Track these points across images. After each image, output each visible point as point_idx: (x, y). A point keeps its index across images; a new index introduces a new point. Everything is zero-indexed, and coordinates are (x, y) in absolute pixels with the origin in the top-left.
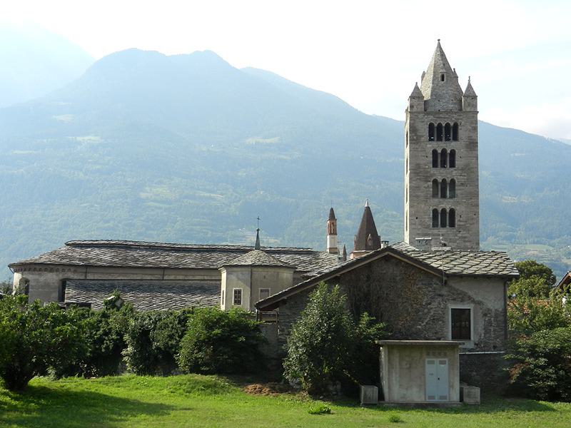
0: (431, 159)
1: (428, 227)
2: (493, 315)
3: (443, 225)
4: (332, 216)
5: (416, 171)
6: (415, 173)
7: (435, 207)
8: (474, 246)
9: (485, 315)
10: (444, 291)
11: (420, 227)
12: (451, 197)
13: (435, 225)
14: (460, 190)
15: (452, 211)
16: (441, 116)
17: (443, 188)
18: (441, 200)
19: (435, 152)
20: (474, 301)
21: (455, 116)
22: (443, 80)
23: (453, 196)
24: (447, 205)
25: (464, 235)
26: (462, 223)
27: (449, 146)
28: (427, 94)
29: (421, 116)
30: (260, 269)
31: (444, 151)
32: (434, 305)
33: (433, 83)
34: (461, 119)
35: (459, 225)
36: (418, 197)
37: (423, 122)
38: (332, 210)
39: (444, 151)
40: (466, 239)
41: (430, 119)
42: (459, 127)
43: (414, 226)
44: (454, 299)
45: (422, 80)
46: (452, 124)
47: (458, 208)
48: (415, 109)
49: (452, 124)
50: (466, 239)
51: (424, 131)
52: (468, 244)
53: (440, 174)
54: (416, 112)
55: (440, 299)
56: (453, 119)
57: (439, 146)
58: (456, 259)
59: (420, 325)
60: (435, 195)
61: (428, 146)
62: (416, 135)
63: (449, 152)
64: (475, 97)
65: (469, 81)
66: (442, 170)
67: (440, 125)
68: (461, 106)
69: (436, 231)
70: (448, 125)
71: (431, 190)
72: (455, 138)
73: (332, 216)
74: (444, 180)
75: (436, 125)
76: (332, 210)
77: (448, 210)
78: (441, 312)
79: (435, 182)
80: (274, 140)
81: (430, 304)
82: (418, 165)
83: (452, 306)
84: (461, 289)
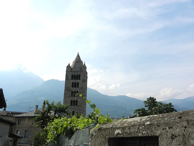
0: (72, 85)
3: (74, 105)
15: (77, 101)
19: (73, 83)
21: (79, 72)
27: (77, 81)
29: (69, 72)
31: (76, 82)
35: (79, 105)
36: (67, 96)
39: (76, 82)
40: (80, 110)
48: (68, 70)
50: (80, 110)
51: (70, 77)
52: (81, 111)
53: (74, 89)
54: (68, 71)
57: (74, 81)
60: (72, 96)
64: (86, 67)
69: (71, 107)
70: (77, 75)
71: (71, 94)
72: (79, 79)
75: (74, 75)
77: (75, 100)
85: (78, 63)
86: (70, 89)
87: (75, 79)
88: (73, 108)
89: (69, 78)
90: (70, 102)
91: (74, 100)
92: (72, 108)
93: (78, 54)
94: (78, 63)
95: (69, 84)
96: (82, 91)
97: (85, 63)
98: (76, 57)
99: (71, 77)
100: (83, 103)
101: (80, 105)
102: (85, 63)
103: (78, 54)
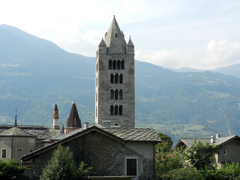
0: (110, 79)
1: (108, 115)
2: (148, 162)
3: (116, 114)
4: (56, 109)
5: (102, 85)
6: (101, 86)
7: (111, 105)
8: (132, 125)
9: (144, 162)
10: (123, 150)
11: (104, 115)
12: (120, 99)
13: (112, 114)
14: (125, 95)
15: (121, 107)
16: (115, 56)
17: (116, 94)
18: (115, 101)
19: (112, 75)
20: (138, 155)
21: (123, 56)
22: (116, 37)
23: (121, 99)
24: (118, 103)
25: (127, 120)
26: (125, 113)
27: (120, 72)
28: (108, 44)
29: (105, 56)
30: (17, 138)
31: (117, 75)
32: (118, 157)
33: (111, 38)
34: (126, 58)
35: (125, 114)
36: (103, 99)
37: (106, 59)
38: (56, 105)
39: (117, 75)
40: (128, 122)
41: (110, 58)
42: (125, 62)
43: (101, 115)
44: (128, 154)
45: (105, 36)
46: (121, 60)
47: (124, 105)
48: (102, 52)
49: (121, 60)
51: (107, 64)
52: (129, 124)
53: (115, 87)
54: (102, 54)
55: (121, 154)
56: (122, 58)
57: (115, 72)
58: (129, 133)
59: (110, 168)
60: (112, 98)
61: (108, 72)
62: (102, 66)
63: (119, 75)
64: (133, 47)
65: (130, 38)
66: (116, 85)
67: (115, 61)
68: (126, 51)
69: (112, 117)
70: (119, 61)
71: (110, 95)
72: (123, 68)
73: (56, 109)
74: (117, 90)
75: (113, 61)
76: (56, 105)
77: (119, 106)
78: (121, 161)
79: (112, 91)
80: (17, 65)
81: (115, 156)
82: (103, 82)
83: (127, 157)
84: (131, 148)
88: (115, 119)
89: (106, 66)
91: (116, 106)
92: (114, 119)
96: (129, 90)
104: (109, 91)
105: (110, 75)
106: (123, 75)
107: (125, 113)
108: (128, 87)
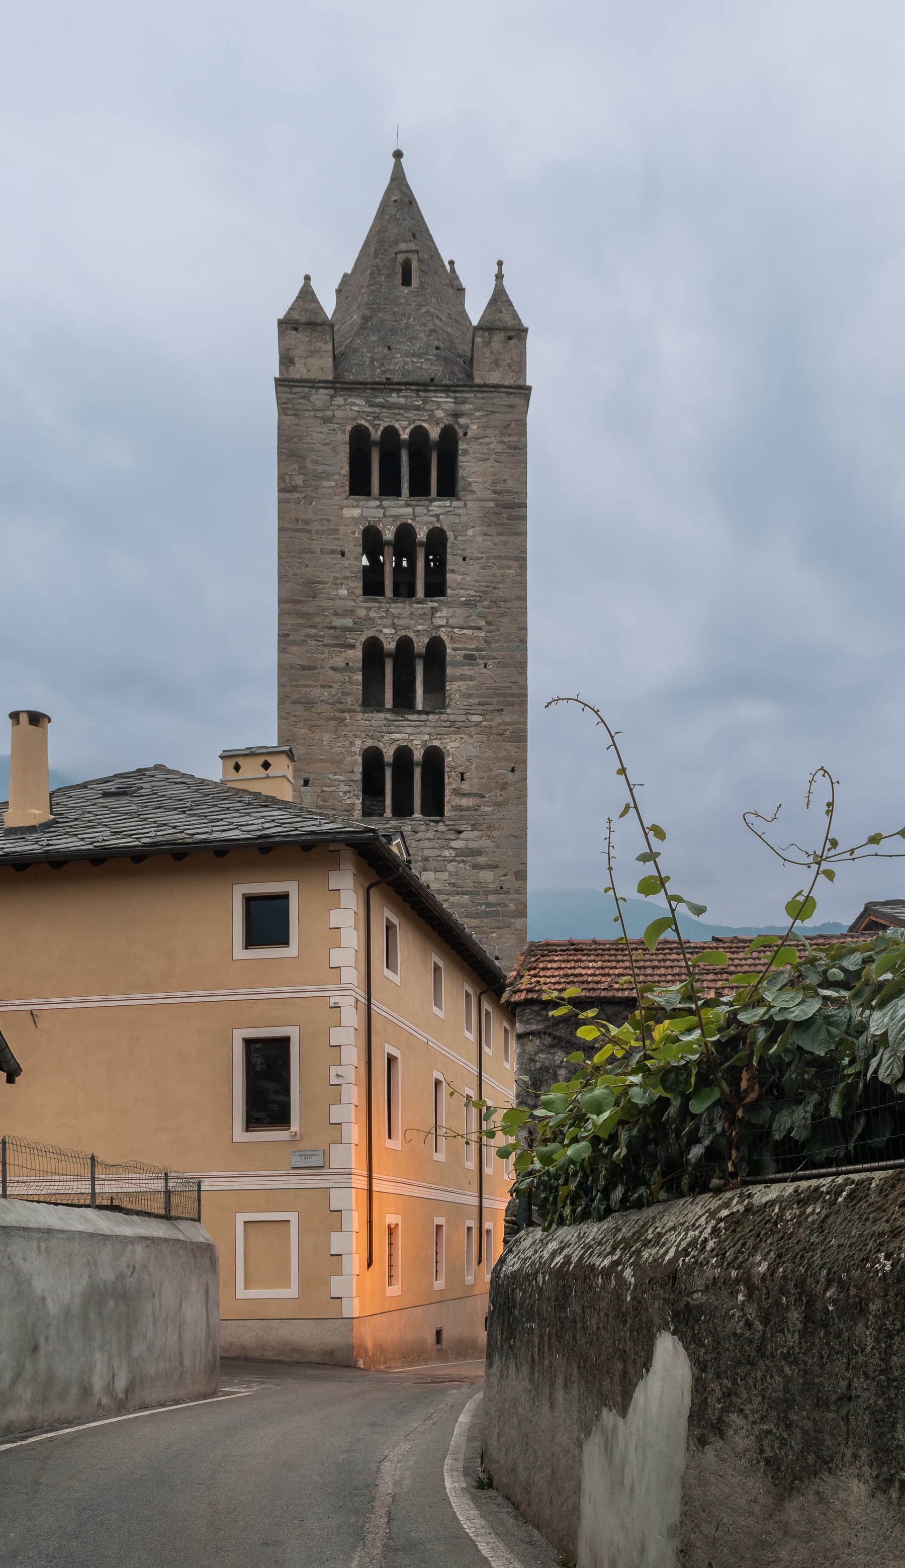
7: (370, 743)
8: (510, 882)
14: (462, 678)
25: (474, 845)
26: (465, 802)
29: (320, 397)
31: (405, 532)
35: (460, 808)
36: (309, 704)
37: (327, 420)
39: (405, 532)
40: (481, 860)
42: (462, 446)
46: (434, 433)
48: (299, 371)
49: (434, 433)
50: (481, 860)
52: (487, 876)
54: (302, 382)
56: (440, 414)
66: (397, 608)
70: (419, 433)
71: (359, 677)
74: (405, 644)
75: (376, 435)
77: (418, 755)
79: (373, 649)
85: (415, 282)
86: (348, 622)
87: (390, 489)
89: (328, 476)
90: (359, 769)
91: (403, 754)
93: (398, 179)
94: (407, 281)
95: (333, 552)
97: (499, 277)
98: (381, 197)
99: (342, 465)
100: (504, 787)
101: (477, 808)
102: (499, 277)
103: (398, 179)
104: (350, 652)
105: (358, 535)
106: (450, 534)
107: (465, 802)
108: (482, 623)
